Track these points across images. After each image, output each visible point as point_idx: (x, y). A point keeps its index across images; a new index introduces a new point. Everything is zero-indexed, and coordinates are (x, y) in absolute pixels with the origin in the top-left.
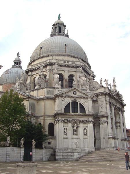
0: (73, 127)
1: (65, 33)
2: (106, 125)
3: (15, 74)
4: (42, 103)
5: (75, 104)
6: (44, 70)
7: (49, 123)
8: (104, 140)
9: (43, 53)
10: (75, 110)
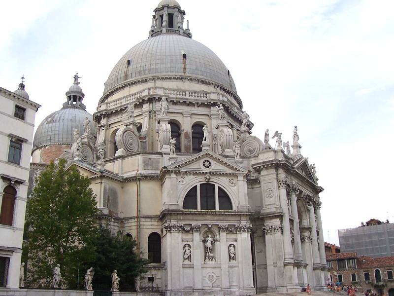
0: (205, 241)
1: (182, 29)
2: (279, 234)
3: (70, 124)
4: (132, 188)
5: (208, 188)
6: (137, 112)
7: (149, 232)
8: (276, 270)
9: (134, 75)
10: (208, 203)
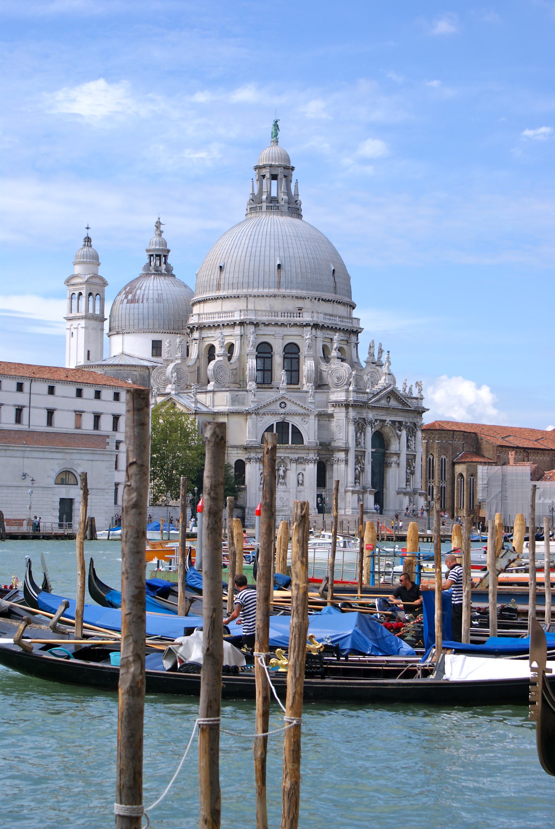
2: (342, 466)
3: (156, 305)
5: (283, 426)
